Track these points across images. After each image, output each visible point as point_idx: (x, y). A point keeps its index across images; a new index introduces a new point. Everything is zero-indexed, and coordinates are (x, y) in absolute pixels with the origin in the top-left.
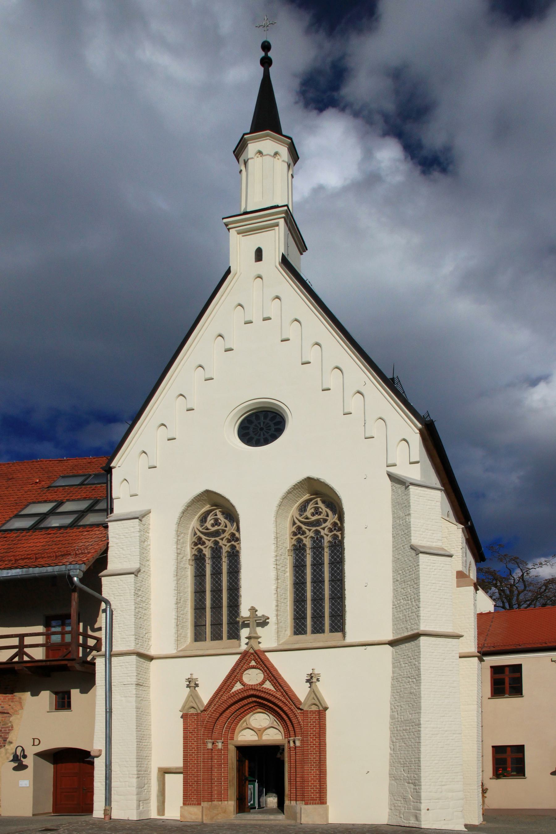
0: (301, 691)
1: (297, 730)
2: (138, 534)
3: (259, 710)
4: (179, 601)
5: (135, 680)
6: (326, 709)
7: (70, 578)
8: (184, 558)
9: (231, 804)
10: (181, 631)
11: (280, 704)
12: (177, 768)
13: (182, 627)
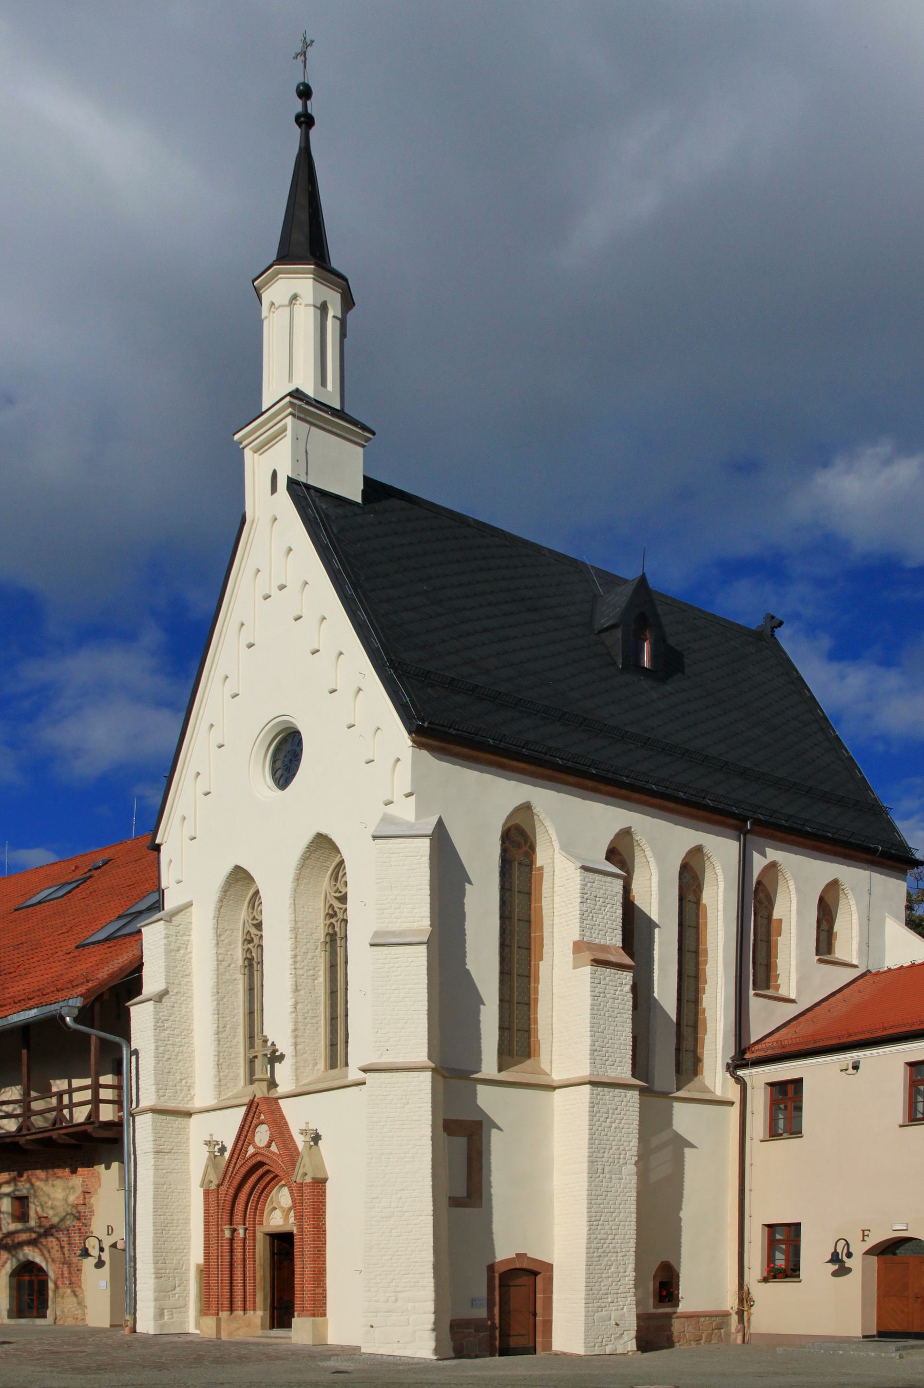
2: (164, 941)
4: (221, 1029)
5: (151, 1146)
7: (63, 1018)
8: (232, 966)
9: (258, 1315)
10: (227, 1071)
13: (229, 1065)
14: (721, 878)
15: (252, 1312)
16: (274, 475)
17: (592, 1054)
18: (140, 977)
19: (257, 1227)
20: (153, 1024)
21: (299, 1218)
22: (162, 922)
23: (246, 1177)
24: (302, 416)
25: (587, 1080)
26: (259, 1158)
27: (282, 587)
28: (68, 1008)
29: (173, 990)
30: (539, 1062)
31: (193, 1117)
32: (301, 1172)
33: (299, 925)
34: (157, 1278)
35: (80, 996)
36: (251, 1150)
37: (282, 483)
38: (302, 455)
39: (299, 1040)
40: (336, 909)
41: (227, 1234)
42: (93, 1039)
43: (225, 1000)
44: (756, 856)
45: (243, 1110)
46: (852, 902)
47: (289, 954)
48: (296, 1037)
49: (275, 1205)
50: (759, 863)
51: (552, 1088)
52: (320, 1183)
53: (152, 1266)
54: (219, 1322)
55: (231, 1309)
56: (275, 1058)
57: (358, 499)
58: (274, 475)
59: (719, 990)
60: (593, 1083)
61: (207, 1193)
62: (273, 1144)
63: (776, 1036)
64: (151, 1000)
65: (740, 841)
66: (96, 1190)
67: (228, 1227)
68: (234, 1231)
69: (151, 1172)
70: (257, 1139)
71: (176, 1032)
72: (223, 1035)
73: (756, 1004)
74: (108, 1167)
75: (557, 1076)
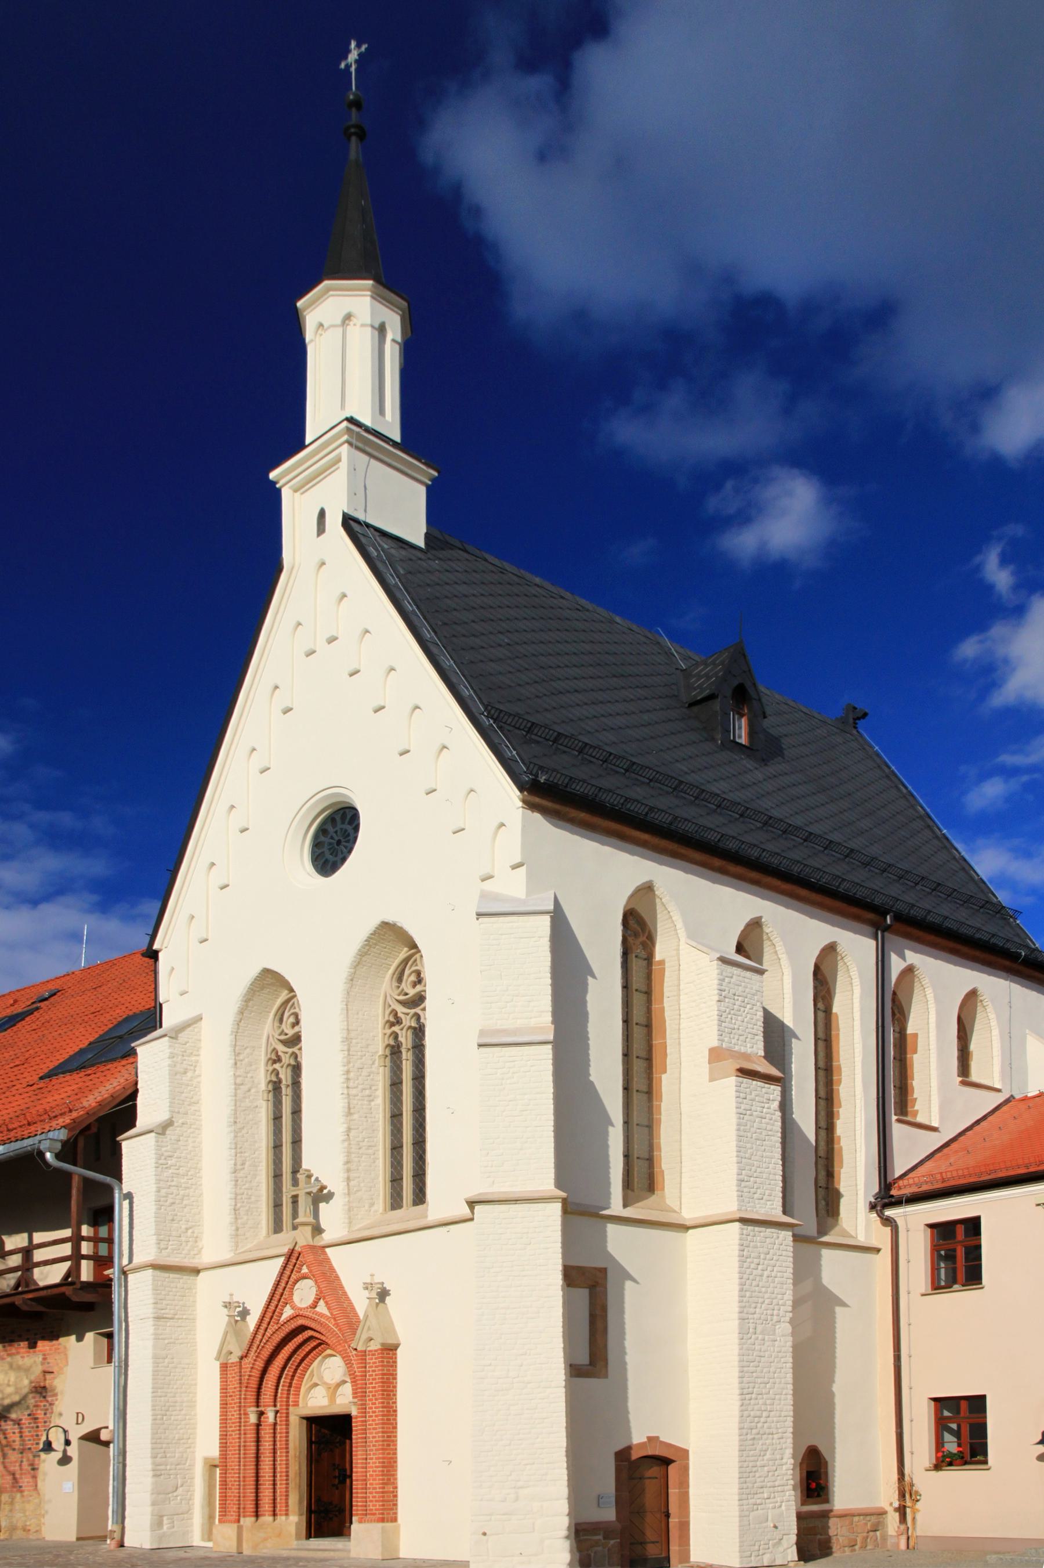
14: (856, 981)
15: (284, 1518)
16: (322, 514)
17: (739, 1185)
18: (135, 1106)
19: (291, 1408)
20: (154, 1161)
21: (360, 1393)
22: (166, 1039)
23: (284, 1346)
24: (360, 445)
25: (738, 1216)
26: (301, 1322)
27: (332, 640)
28: (48, 1146)
29: (178, 1121)
30: (663, 1197)
31: (201, 1274)
32: (364, 1337)
33: (353, 1034)
34: (155, 1476)
35: (64, 1127)
36: (288, 1312)
37: (334, 522)
38: (359, 488)
39: (352, 1175)
40: (400, 1015)
41: (253, 1419)
42: (75, 1182)
43: (244, 1131)
44: (894, 957)
45: (281, 1261)
46: (992, 1016)
47: (341, 1070)
48: (348, 1170)
49: (315, 1380)
50: (896, 965)
51: (686, 1228)
52: (390, 1350)
53: (149, 1461)
54: (240, 1529)
55: (257, 1515)
56: (321, 1196)
57: (421, 543)
58: (322, 514)
59: (858, 1115)
60: (744, 1221)
61: (224, 1367)
62: (322, 1303)
63: (921, 1170)
64: (152, 1131)
65: (876, 939)
66: (61, 1369)
67: (255, 1409)
68: (261, 1414)
69: (150, 1343)
70: (296, 1298)
71: (181, 1171)
72: (241, 1174)
73: (898, 1131)
74: (80, 1339)
75: (688, 1214)
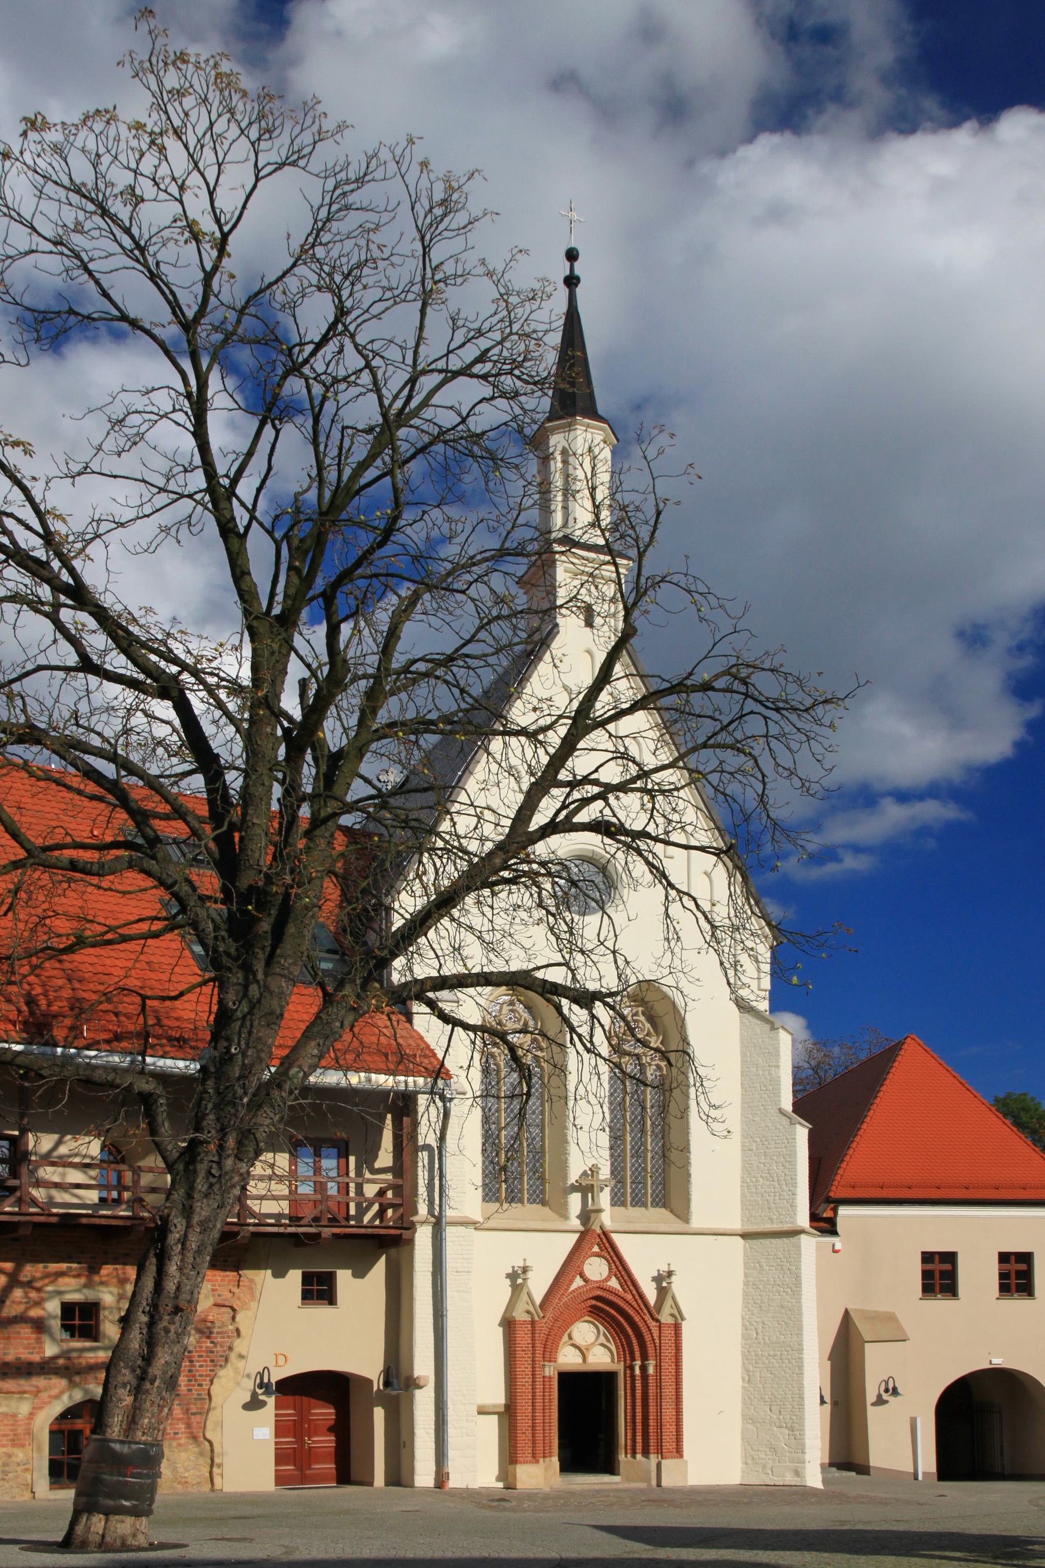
0: (651, 1294)
1: (651, 1351)
3: (587, 1318)
6: (683, 1319)
11: (631, 1312)
12: (495, 1406)
